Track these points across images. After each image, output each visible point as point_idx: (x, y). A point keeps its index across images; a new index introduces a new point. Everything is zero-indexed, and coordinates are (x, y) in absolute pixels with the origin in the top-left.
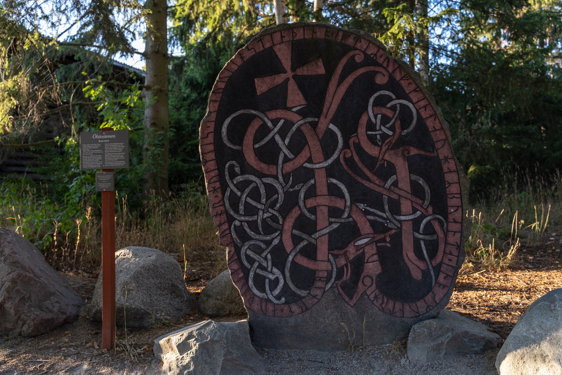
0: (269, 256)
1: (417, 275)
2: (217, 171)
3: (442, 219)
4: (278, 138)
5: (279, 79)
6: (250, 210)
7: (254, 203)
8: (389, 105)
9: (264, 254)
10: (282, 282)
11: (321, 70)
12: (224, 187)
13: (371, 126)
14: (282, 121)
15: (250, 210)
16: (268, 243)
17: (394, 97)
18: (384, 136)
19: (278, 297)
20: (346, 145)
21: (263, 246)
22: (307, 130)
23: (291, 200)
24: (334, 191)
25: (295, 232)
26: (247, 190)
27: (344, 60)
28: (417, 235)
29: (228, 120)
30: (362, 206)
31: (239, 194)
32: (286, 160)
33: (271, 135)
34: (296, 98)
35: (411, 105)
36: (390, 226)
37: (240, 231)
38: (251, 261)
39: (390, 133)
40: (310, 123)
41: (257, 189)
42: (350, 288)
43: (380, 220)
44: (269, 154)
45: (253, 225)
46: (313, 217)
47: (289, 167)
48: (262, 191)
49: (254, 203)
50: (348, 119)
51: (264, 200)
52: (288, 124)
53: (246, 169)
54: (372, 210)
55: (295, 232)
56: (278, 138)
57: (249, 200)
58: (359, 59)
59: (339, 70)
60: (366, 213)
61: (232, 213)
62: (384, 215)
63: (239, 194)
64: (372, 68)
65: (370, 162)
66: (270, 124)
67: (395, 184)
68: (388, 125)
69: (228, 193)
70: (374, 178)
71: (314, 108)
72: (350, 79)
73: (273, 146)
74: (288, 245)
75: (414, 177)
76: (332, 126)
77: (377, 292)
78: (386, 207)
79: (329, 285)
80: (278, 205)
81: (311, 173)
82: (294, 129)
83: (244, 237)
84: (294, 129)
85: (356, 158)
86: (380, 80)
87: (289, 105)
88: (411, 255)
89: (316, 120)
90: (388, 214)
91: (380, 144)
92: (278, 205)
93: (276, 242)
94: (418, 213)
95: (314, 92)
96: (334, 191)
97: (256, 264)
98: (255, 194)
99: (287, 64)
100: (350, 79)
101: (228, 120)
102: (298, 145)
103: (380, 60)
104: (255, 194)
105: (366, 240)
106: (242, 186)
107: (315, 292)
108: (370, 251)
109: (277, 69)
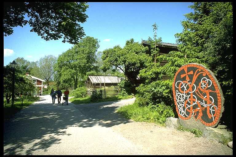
3: (215, 106)
4: (184, 86)
5: (185, 75)
6: (180, 99)
12: (176, 95)
15: (180, 99)
16: (182, 106)
17: (207, 79)
18: (204, 87)
21: (181, 106)
23: (186, 98)
24: (194, 98)
26: (179, 96)
27: (197, 71)
28: (210, 109)
29: (177, 83)
30: (199, 101)
32: (186, 91)
33: (183, 86)
34: (188, 79)
35: (211, 81)
37: (178, 102)
39: (206, 87)
45: (180, 102)
48: (182, 96)
50: (197, 82)
51: (182, 97)
53: (179, 92)
54: (201, 103)
56: (184, 86)
60: (200, 103)
61: (177, 99)
65: (201, 92)
67: (206, 97)
68: (205, 85)
69: (176, 96)
70: (201, 95)
71: (191, 81)
72: (198, 75)
73: (183, 88)
74: (186, 106)
75: (210, 97)
76: (194, 85)
79: (192, 116)
80: (184, 99)
81: (190, 94)
83: (179, 104)
86: (204, 75)
90: (204, 104)
92: (184, 99)
93: (183, 106)
94: (211, 105)
95: (191, 77)
98: (180, 96)
100: (198, 75)
101: (177, 83)
102: (188, 88)
103: (204, 71)
104: (180, 96)
105: (199, 108)
106: (178, 95)
108: (200, 111)
109: (185, 73)
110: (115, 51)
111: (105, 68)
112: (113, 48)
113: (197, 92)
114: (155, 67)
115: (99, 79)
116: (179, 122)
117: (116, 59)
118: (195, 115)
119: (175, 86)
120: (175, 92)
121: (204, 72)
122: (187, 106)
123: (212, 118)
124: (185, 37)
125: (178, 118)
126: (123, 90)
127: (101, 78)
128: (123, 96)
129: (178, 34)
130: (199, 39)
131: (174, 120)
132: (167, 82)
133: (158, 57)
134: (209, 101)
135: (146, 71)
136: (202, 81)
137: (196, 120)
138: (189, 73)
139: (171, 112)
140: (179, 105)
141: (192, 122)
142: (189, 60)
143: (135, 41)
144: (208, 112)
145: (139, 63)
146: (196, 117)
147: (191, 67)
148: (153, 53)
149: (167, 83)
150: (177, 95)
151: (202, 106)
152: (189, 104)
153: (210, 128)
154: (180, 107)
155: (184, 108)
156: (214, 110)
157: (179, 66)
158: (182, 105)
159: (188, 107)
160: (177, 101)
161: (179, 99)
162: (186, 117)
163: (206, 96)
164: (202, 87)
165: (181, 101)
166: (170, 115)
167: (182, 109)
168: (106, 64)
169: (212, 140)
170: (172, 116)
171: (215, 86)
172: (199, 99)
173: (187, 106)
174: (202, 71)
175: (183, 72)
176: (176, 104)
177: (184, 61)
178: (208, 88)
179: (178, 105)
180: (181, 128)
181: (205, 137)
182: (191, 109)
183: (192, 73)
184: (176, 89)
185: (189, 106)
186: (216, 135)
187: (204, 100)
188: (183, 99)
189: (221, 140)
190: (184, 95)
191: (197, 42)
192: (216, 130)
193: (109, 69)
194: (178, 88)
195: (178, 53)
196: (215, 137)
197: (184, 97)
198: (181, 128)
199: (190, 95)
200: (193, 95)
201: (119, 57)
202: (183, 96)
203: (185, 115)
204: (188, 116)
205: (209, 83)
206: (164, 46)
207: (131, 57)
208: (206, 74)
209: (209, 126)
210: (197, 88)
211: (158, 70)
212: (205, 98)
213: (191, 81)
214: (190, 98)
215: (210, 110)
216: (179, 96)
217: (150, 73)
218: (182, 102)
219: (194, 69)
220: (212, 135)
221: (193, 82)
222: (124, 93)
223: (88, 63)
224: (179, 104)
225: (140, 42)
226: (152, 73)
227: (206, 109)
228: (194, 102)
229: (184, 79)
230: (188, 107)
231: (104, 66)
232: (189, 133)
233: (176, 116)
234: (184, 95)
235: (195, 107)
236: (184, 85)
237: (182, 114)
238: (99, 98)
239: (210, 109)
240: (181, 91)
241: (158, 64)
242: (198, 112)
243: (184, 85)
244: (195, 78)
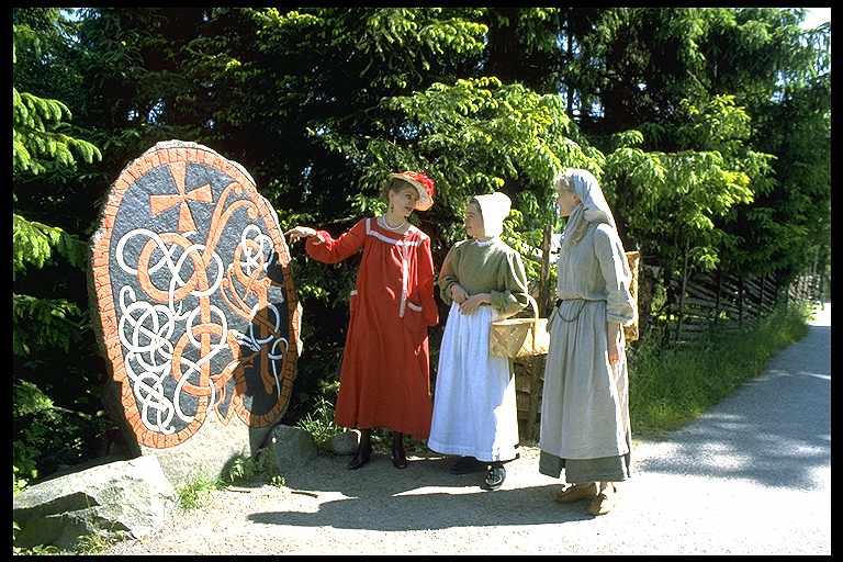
1: (269, 390)
7: (148, 333)
9: (155, 387)
11: (209, 199)
12: (119, 315)
14: (175, 246)
15: (145, 341)
18: (253, 269)
22: (197, 258)
23: (181, 325)
24: (215, 319)
27: (227, 192)
28: (270, 356)
29: (123, 241)
31: (132, 321)
32: (177, 287)
34: (186, 223)
36: (254, 349)
38: (145, 395)
39: (256, 264)
40: (199, 251)
41: (150, 318)
42: (223, 410)
44: (161, 280)
47: (181, 294)
49: (148, 333)
51: (156, 330)
53: (142, 296)
55: (185, 361)
56: (170, 263)
58: (239, 191)
59: (223, 197)
61: (125, 342)
62: (248, 339)
63: (132, 321)
65: (241, 290)
66: (164, 249)
70: (244, 306)
72: (229, 212)
80: (169, 336)
86: (253, 215)
88: (267, 374)
92: (169, 336)
93: (167, 373)
96: (215, 319)
97: (149, 397)
98: (148, 324)
100: (229, 212)
101: (123, 241)
102: (187, 273)
104: (148, 324)
106: (136, 315)
107: (198, 417)
118: (222, 399)
119: (113, 266)
120: (116, 300)
122: (184, 368)
136: (244, 238)
140: (143, 376)
144: (264, 364)
146: (223, 410)
147: (203, 165)
154: (146, 388)
155: (170, 384)
158: (162, 367)
165: (151, 349)
167: (160, 396)
173: (184, 368)
176: (121, 372)
179: (134, 377)
182: (205, 378)
183: (205, 193)
188: (163, 336)
190: (169, 312)
194: (134, 272)
197: (171, 325)
199: (196, 312)
200: (214, 308)
202: (163, 319)
210: (225, 269)
213: (200, 238)
214: (197, 322)
216: (137, 325)
221: (209, 241)
228: (215, 340)
229: (169, 222)
230: (189, 372)
234: (169, 312)
236: (167, 259)
239: (270, 356)
243: (167, 259)
244: (219, 224)
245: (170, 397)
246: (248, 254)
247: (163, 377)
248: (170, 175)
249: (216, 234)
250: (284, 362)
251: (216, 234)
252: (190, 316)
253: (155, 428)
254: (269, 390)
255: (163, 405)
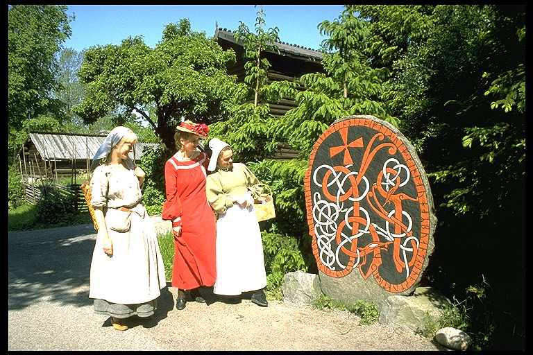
0: (330, 245)
1: (400, 270)
2: (310, 197)
4: (338, 183)
5: (342, 148)
6: (324, 220)
8: (394, 168)
9: (327, 243)
10: (334, 258)
12: (313, 205)
13: (384, 180)
15: (324, 220)
16: (330, 238)
17: (398, 163)
18: (390, 186)
19: (332, 267)
20: (370, 190)
21: (328, 239)
23: (342, 215)
25: (343, 235)
26: (323, 209)
30: (375, 226)
32: (341, 194)
34: (348, 159)
36: (388, 239)
37: (318, 228)
38: (322, 246)
39: (393, 184)
43: (383, 235)
45: (324, 227)
46: (351, 228)
50: (373, 174)
51: (329, 215)
52: (344, 175)
53: (323, 198)
55: (343, 235)
57: (324, 214)
60: (377, 229)
64: (386, 144)
65: (382, 200)
66: (335, 174)
67: (393, 215)
68: (393, 180)
69: (314, 209)
72: (375, 151)
73: (335, 186)
74: (339, 240)
75: (404, 213)
76: (364, 178)
77: (378, 274)
78: (387, 228)
80: (335, 219)
82: (346, 177)
83: (320, 233)
84: (346, 177)
85: (375, 196)
86: (392, 151)
87: (345, 164)
89: (356, 173)
91: (388, 190)
92: (335, 219)
93: (333, 238)
94: (404, 235)
97: (324, 248)
98: (326, 211)
99: (345, 141)
100: (375, 151)
102: (347, 187)
104: (326, 211)
106: (321, 206)
110: (125, 56)
111: (91, 110)
112: (119, 44)
113: (372, 199)
114: (255, 116)
115: (70, 146)
116: (319, 285)
117: (128, 83)
118: (364, 263)
120: (312, 199)
121: (393, 143)
122: (343, 239)
123: (404, 269)
124: (348, 34)
125: (317, 273)
126: (151, 185)
127: (76, 143)
128: (150, 204)
129: (327, 24)
130: (381, 44)
131: (304, 279)
132: (290, 165)
133: (265, 87)
134: (399, 225)
135: (226, 129)
136: (384, 168)
137: (366, 277)
138: (352, 145)
139: (297, 255)
140: (322, 236)
141: (355, 284)
142: (354, 104)
143: (195, 28)
144: (396, 254)
145: (204, 102)
146: (365, 269)
148: (249, 74)
149: (291, 171)
150: (316, 206)
151: (382, 239)
152: (349, 234)
153: (400, 298)
155: (334, 246)
156: (411, 250)
157: (328, 119)
158: (330, 235)
159: (345, 241)
160: (315, 223)
161: (323, 218)
162: (338, 269)
163: (393, 212)
164: (384, 187)
165: (326, 224)
166: (295, 264)
168: (94, 99)
169: (401, 328)
170: (301, 269)
171: (416, 183)
172: (375, 219)
174: (386, 140)
175: (335, 139)
176: (314, 232)
177: (340, 106)
178: (400, 190)
179: (318, 236)
180: (323, 302)
181: (385, 322)
183: (359, 143)
184: (314, 188)
185: (348, 239)
186: (410, 315)
187: (387, 223)
188: (333, 219)
189: (422, 328)
190: (337, 207)
191: (375, 52)
192: (412, 302)
193: (102, 113)
195: (328, 81)
196: (408, 319)
197: (337, 214)
198: (323, 301)
199: (352, 208)
200: (361, 209)
201: (141, 77)
202: (333, 210)
203: (335, 265)
204: (343, 267)
205: (403, 177)
206: (284, 52)
207: (180, 82)
208: (396, 149)
209: (397, 293)
211: (263, 126)
212: (389, 216)
214: (351, 215)
215: (401, 250)
216: (321, 211)
217: (240, 136)
218: (331, 226)
219: (366, 133)
220: (402, 316)
221: (361, 170)
222: (153, 195)
223: (27, 89)
224: (320, 233)
225: (210, 34)
226: (246, 136)
227: (391, 246)
228: (362, 227)
229: (338, 160)
230: (345, 241)
231: (89, 103)
232: (343, 316)
233: (313, 268)
234: (337, 207)
235: (364, 241)
236: (336, 179)
237: (328, 262)
238: (68, 211)
240: (328, 196)
241: (266, 108)
242: (370, 257)
243: (336, 179)
245: (334, 250)
246: (387, 177)
247: (331, 240)
248: (340, 136)
249: (365, 165)
250: (415, 254)
251: (365, 165)
252: (348, 211)
253: (325, 264)
254: (400, 270)
255: (330, 254)
